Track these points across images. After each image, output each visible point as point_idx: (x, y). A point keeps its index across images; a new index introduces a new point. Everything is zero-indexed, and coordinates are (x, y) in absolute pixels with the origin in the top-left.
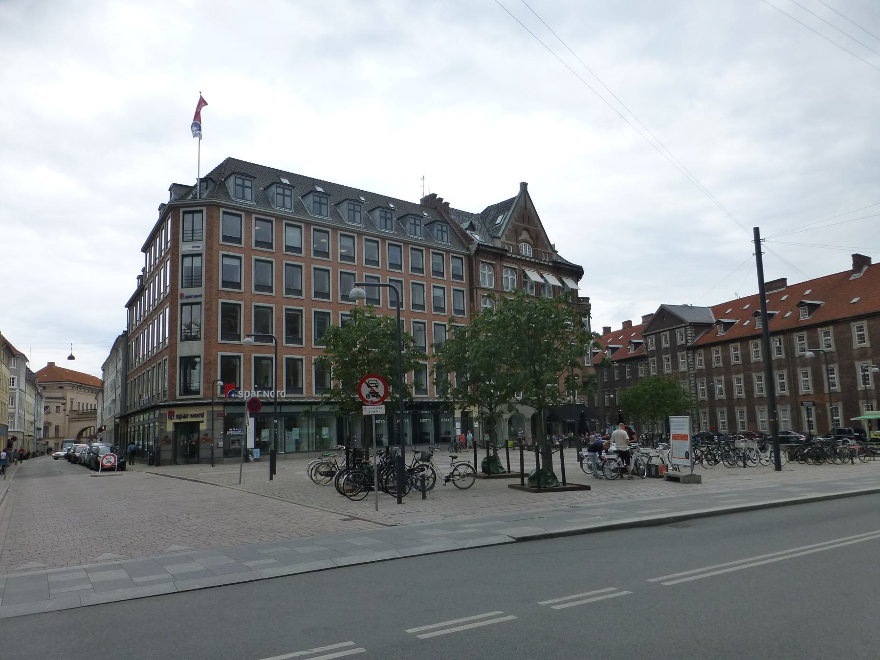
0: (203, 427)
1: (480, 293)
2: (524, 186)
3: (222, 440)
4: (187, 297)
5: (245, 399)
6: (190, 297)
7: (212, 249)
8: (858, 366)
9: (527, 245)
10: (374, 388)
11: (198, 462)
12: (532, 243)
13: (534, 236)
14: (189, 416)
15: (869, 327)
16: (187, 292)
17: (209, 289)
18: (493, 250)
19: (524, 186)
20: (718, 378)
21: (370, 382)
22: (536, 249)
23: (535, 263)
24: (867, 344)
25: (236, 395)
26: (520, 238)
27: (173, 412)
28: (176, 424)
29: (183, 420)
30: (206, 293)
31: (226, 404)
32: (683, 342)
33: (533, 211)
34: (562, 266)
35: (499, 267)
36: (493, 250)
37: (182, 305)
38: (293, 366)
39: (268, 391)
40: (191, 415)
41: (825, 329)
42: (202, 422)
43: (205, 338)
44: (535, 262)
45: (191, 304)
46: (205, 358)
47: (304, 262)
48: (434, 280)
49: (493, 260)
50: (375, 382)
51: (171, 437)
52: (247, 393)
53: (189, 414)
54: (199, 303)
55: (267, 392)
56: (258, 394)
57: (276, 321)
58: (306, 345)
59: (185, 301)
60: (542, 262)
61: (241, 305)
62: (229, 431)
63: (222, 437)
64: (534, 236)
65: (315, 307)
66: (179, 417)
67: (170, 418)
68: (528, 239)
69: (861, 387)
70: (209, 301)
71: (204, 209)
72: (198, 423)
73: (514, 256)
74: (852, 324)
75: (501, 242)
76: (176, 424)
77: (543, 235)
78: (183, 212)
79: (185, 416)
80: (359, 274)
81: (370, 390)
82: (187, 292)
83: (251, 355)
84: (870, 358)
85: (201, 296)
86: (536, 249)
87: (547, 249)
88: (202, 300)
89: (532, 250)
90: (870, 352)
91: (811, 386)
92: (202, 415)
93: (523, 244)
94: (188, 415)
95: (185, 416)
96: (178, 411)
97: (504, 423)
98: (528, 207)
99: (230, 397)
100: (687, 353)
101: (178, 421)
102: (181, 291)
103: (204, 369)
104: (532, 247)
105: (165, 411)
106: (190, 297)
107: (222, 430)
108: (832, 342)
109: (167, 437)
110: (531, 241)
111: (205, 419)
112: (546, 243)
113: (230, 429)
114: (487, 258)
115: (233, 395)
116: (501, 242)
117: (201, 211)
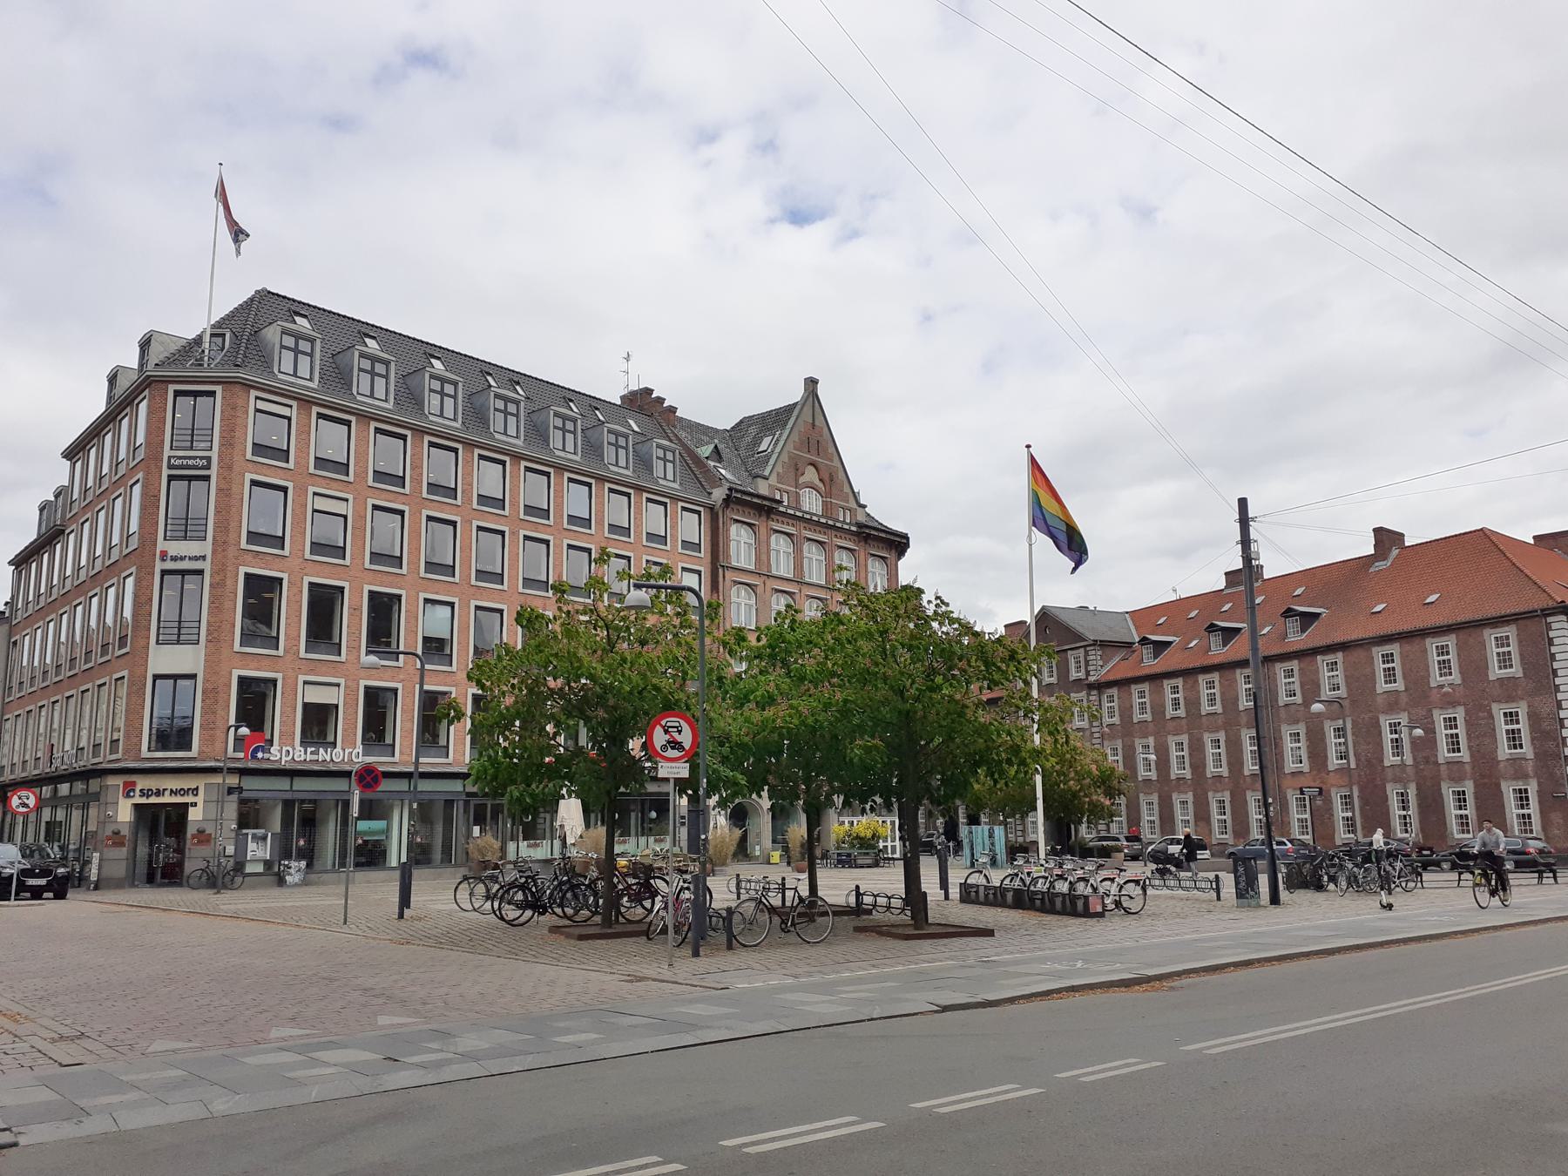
0: (195, 815)
1: (730, 575)
2: (811, 383)
3: (232, 841)
4: (174, 559)
5: (283, 763)
6: (182, 559)
7: (230, 468)
8: (1385, 722)
9: (814, 492)
10: (676, 735)
11: (180, 885)
13: (826, 478)
14: (167, 793)
15: (1404, 657)
16: (175, 548)
17: (220, 545)
18: (755, 500)
19: (811, 383)
20: (1144, 741)
21: (669, 724)
22: (829, 500)
23: (826, 526)
24: (1399, 685)
25: (266, 756)
26: (802, 480)
27: (134, 784)
28: (137, 806)
29: (153, 800)
30: (214, 552)
31: (243, 772)
32: (1082, 675)
35: (763, 530)
36: (755, 500)
37: (164, 573)
39: (329, 750)
40: (172, 790)
41: (1330, 658)
42: (196, 804)
43: (208, 641)
44: (826, 524)
45: (183, 573)
46: (206, 681)
47: (408, 505)
50: (677, 724)
51: (125, 831)
53: (166, 789)
54: (200, 572)
55: (326, 752)
56: (308, 753)
57: (350, 615)
59: (170, 565)
60: (839, 525)
61: (282, 579)
63: (233, 835)
64: (826, 478)
65: (425, 591)
66: (143, 793)
67: (128, 796)
68: (817, 482)
69: (1390, 759)
70: (220, 570)
71: (218, 389)
72: (186, 806)
73: (790, 511)
74: (1375, 650)
75: (770, 485)
76: (137, 806)
77: (841, 474)
78: (175, 391)
79: (159, 793)
80: (512, 533)
81: (667, 737)
82: (175, 548)
83: (297, 678)
84: (1405, 710)
85: (204, 558)
86: (829, 500)
88: (206, 566)
90: (1404, 699)
91: (1305, 759)
92: (195, 791)
93: (807, 490)
94: (164, 790)
95: (159, 793)
96: (142, 783)
97: (764, 816)
98: (817, 423)
99: (254, 757)
100: (1089, 695)
101: (144, 801)
102: (161, 545)
103: (203, 701)
104: (822, 497)
105: (118, 781)
106: (182, 559)
107: (235, 822)
108: (1341, 680)
109: (117, 833)
110: (821, 485)
111: (200, 799)
112: (847, 489)
115: (260, 755)
116: (770, 485)
117: (213, 394)
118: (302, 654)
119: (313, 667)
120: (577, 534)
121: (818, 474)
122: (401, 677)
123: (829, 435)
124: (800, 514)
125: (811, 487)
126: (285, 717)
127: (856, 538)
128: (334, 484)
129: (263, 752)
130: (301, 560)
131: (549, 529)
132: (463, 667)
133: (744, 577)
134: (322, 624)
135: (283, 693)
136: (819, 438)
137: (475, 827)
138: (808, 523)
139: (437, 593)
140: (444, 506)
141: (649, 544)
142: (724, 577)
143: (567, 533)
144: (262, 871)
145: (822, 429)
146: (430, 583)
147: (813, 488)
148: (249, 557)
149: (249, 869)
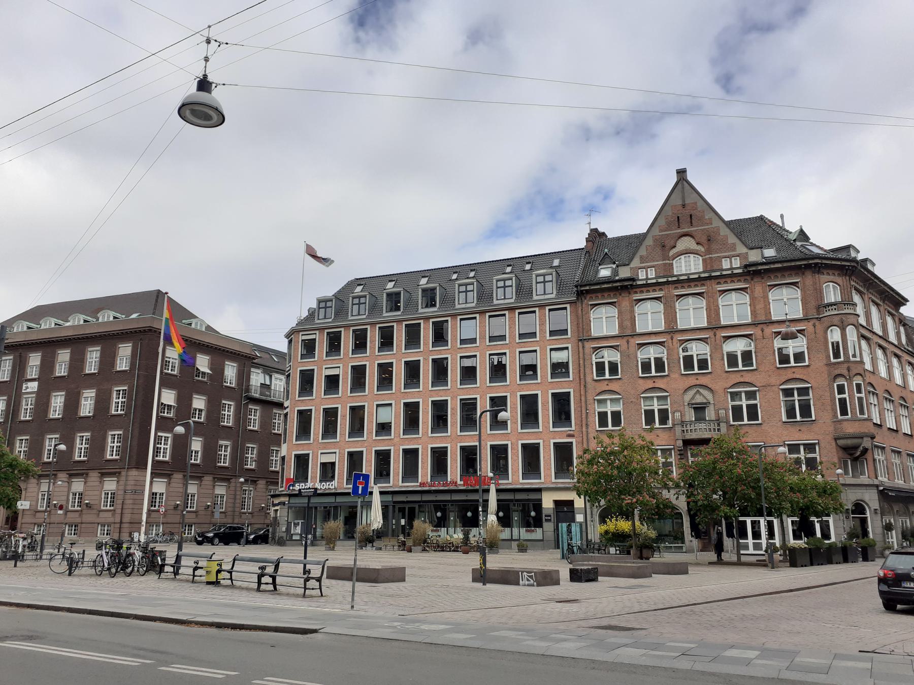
1: (590, 345)
2: (681, 173)
9: (692, 256)
12: (703, 250)
13: (704, 239)
25: (294, 488)
31: (290, 496)
33: (700, 203)
34: (760, 267)
36: (606, 286)
38: (411, 456)
48: (523, 344)
49: (615, 295)
52: (302, 486)
58: (367, 438)
62: (696, 519)
75: (631, 269)
80: (424, 359)
86: (707, 256)
87: (735, 250)
89: (703, 260)
93: (682, 257)
99: (289, 489)
104: (702, 256)
113: (696, 518)
114: (603, 297)
115: (291, 488)
116: (631, 269)
118: (320, 441)
119: (325, 446)
120: (467, 349)
121: (695, 240)
122: (366, 445)
123: (705, 205)
124: (675, 279)
125: (686, 253)
126: (314, 470)
127: (748, 278)
128: (335, 362)
129: (293, 487)
130: (320, 399)
131: (448, 351)
132: (397, 435)
133: (605, 342)
134: (330, 428)
135: (312, 460)
136: (692, 212)
137: (402, 520)
138: (680, 283)
139: (383, 400)
140: (386, 356)
141: (520, 341)
142: (583, 347)
143: (460, 350)
144: (299, 539)
145: (696, 203)
146: (380, 396)
147: (690, 253)
148: (299, 403)
149: (294, 538)
